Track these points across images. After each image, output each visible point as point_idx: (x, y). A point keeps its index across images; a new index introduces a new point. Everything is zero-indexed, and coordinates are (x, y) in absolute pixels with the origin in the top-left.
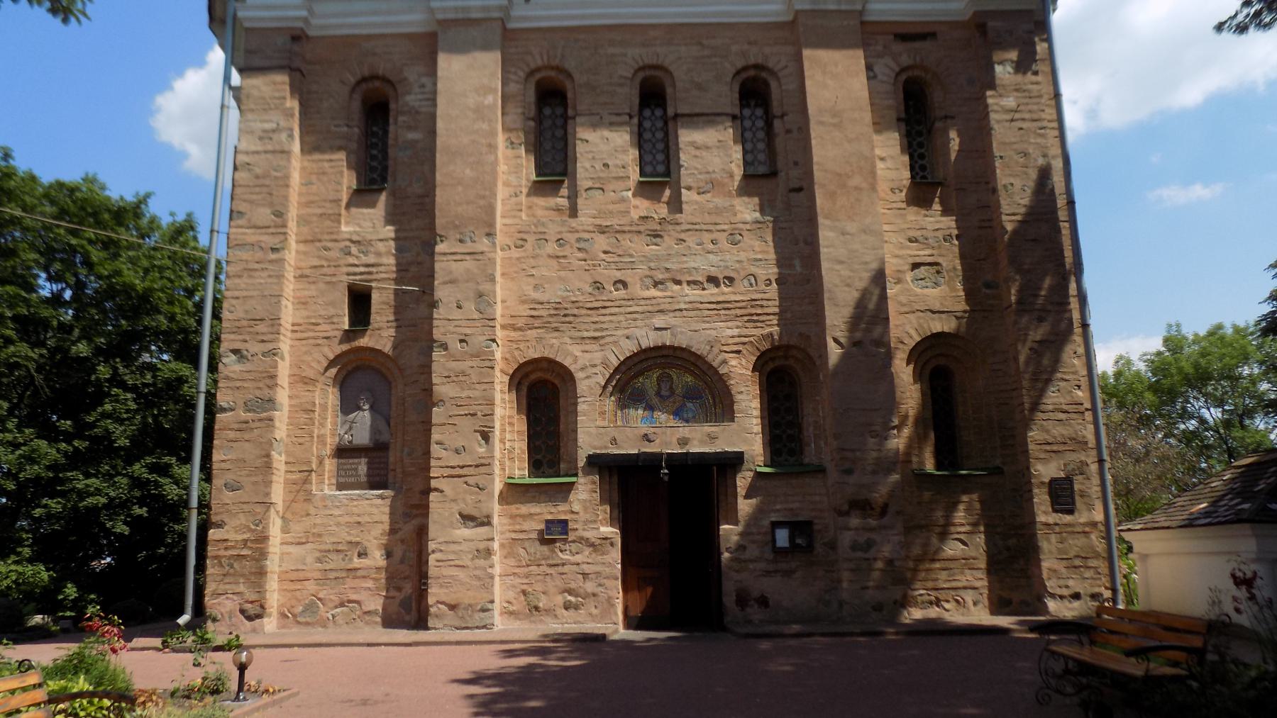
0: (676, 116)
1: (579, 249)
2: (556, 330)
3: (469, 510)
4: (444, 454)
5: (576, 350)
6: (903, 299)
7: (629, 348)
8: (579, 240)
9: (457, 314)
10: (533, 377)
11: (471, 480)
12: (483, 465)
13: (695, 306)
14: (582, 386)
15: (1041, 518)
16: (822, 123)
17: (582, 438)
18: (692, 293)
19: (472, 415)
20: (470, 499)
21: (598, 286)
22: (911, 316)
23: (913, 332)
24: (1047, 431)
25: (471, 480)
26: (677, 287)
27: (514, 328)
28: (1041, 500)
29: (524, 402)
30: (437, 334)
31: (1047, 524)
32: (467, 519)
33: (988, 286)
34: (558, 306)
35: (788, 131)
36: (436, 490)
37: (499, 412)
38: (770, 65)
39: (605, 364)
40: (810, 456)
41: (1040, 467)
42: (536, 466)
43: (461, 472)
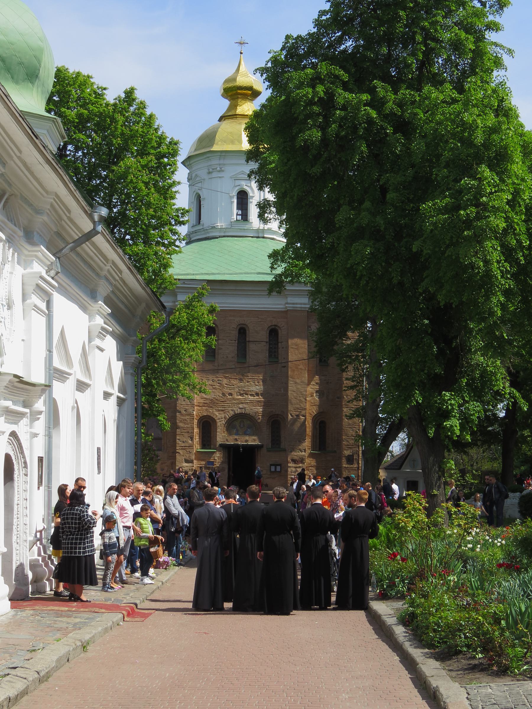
0: (249, 341)
1: (219, 383)
2: (211, 407)
3: (187, 458)
4: (180, 443)
5: (217, 413)
6: (312, 401)
7: (232, 413)
8: (218, 380)
9: (184, 403)
10: (204, 420)
11: (188, 450)
12: (191, 446)
13: (252, 402)
14: (219, 424)
15: (345, 465)
16: (292, 348)
17: (218, 439)
18: (251, 398)
19: (188, 432)
20: (187, 455)
21: (224, 394)
22: (314, 407)
23: (314, 411)
24: (348, 442)
25: (188, 450)
26: (246, 396)
27: (199, 406)
28: (344, 460)
29: (201, 427)
30: (178, 408)
31: (345, 467)
32: (187, 461)
33: (338, 398)
34: (212, 400)
35: (283, 348)
36: (178, 452)
37: (195, 430)
38: (279, 325)
39: (225, 418)
40: (282, 446)
41: (345, 452)
42: (204, 446)
43: (184, 448)
